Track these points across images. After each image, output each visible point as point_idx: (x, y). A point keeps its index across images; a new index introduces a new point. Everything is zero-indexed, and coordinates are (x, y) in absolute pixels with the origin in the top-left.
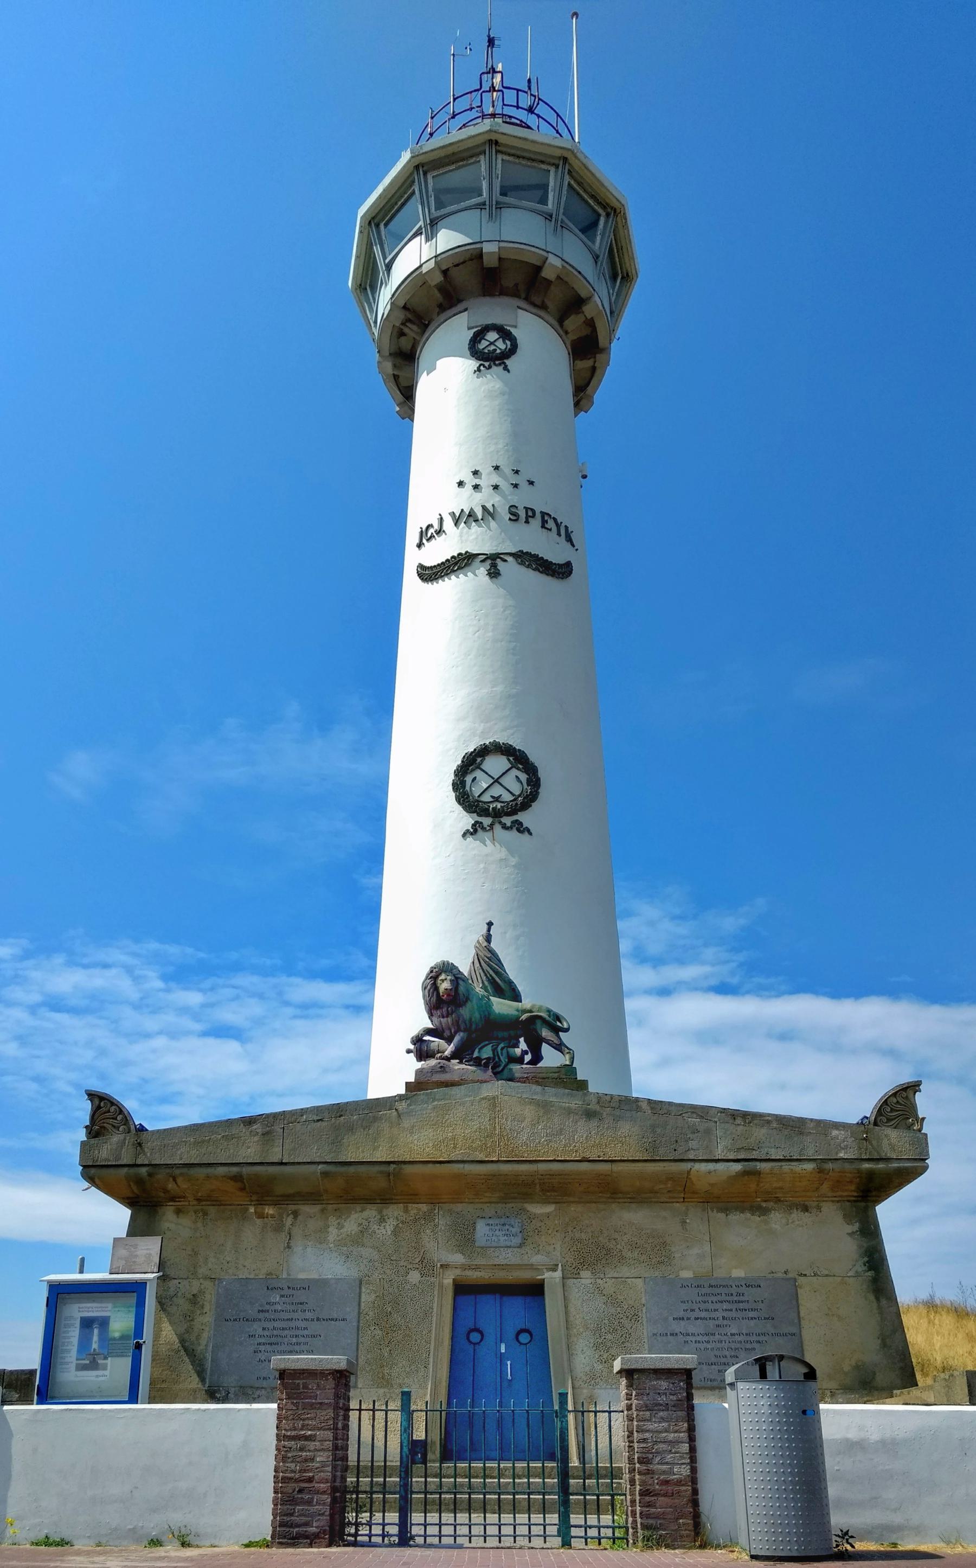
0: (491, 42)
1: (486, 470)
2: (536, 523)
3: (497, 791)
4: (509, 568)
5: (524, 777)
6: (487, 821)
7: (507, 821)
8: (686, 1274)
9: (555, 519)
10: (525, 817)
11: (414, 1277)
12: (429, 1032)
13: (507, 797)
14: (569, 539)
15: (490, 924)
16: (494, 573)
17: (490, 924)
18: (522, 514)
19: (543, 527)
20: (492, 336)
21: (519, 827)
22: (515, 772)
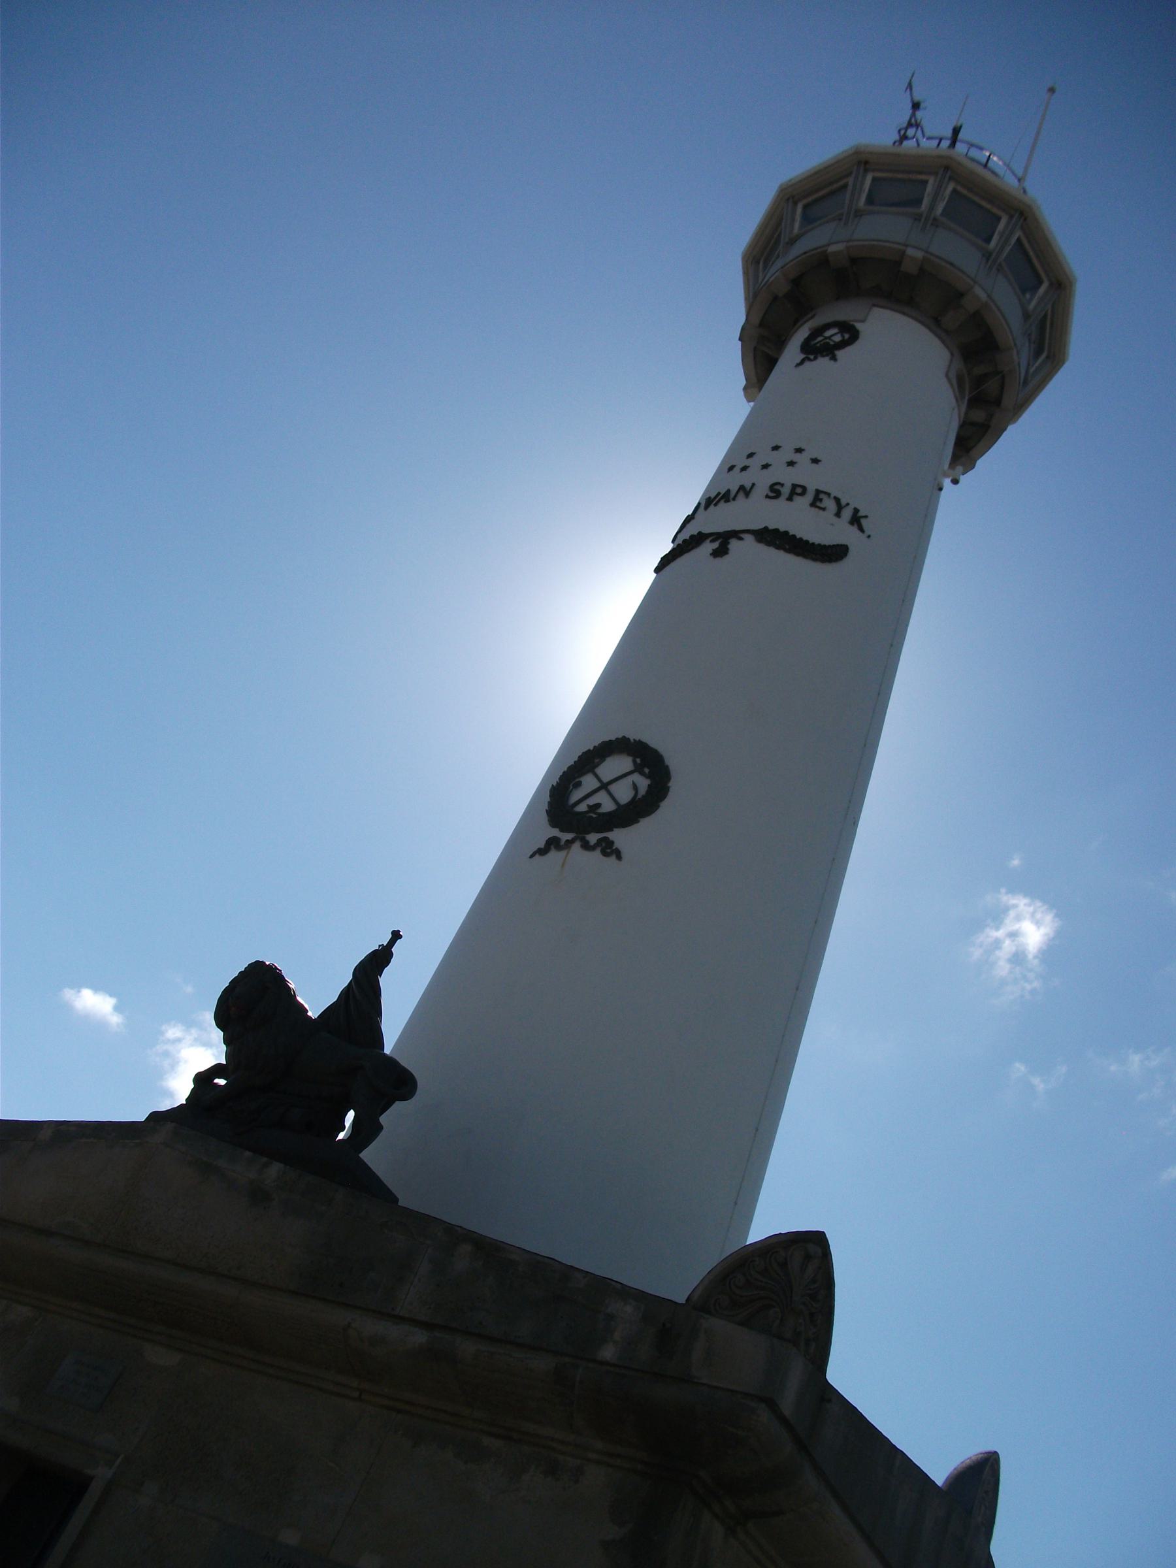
2: (802, 502)
7: (593, 838)
8: (290, 1537)
9: (837, 500)
10: (618, 836)
12: (216, 1070)
13: (608, 806)
15: (396, 935)
17: (396, 935)
18: (786, 491)
19: (813, 505)
21: (609, 849)
22: (637, 778)
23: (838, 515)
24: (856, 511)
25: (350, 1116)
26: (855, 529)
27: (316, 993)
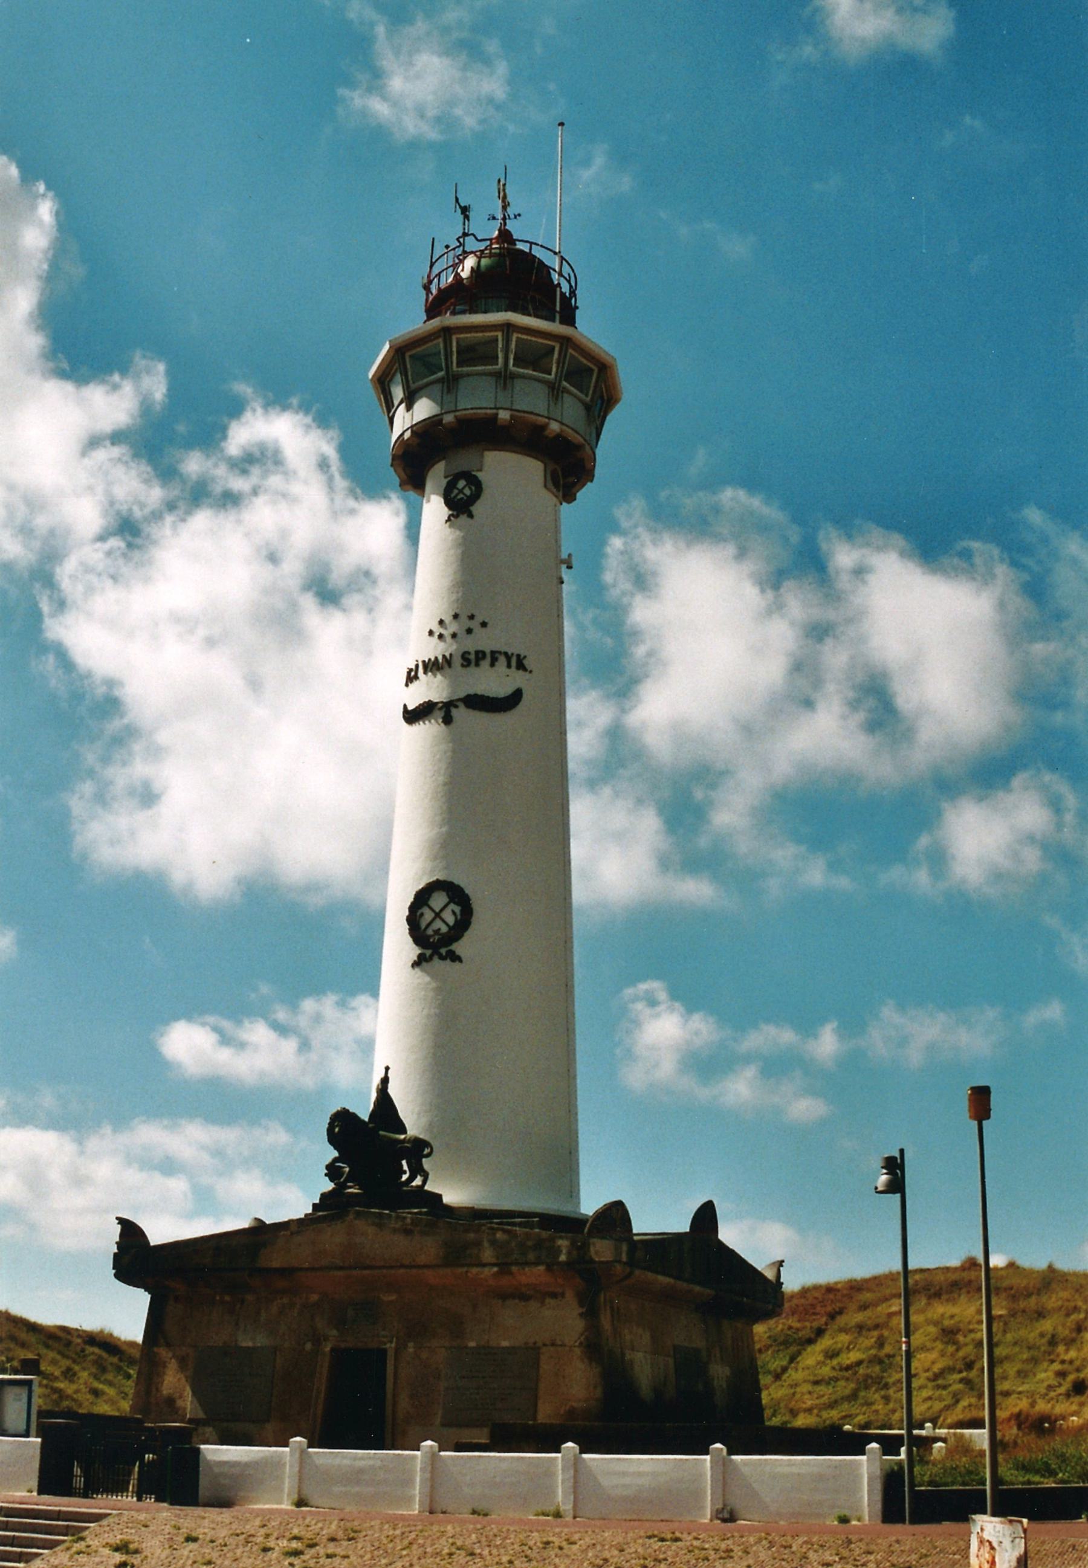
0: (465, 210)
1: (448, 619)
3: (438, 924)
4: (460, 713)
5: (457, 909)
6: (428, 952)
7: (443, 951)
8: (472, 1344)
9: (506, 654)
10: (458, 947)
11: (308, 1346)
12: (335, 1160)
14: (521, 666)
15: (387, 1069)
16: (448, 720)
17: (387, 1069)
18: (472, 657)
20: (461, 484)
21: (455, 958)
22: (452, 906)
23: (509, 666)
24: (518, 656)
25: (404, 1162)
26: (521, 672)
27: (364, 1110)
